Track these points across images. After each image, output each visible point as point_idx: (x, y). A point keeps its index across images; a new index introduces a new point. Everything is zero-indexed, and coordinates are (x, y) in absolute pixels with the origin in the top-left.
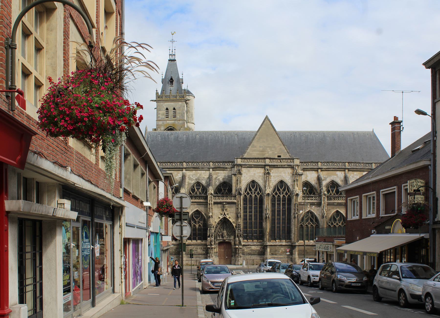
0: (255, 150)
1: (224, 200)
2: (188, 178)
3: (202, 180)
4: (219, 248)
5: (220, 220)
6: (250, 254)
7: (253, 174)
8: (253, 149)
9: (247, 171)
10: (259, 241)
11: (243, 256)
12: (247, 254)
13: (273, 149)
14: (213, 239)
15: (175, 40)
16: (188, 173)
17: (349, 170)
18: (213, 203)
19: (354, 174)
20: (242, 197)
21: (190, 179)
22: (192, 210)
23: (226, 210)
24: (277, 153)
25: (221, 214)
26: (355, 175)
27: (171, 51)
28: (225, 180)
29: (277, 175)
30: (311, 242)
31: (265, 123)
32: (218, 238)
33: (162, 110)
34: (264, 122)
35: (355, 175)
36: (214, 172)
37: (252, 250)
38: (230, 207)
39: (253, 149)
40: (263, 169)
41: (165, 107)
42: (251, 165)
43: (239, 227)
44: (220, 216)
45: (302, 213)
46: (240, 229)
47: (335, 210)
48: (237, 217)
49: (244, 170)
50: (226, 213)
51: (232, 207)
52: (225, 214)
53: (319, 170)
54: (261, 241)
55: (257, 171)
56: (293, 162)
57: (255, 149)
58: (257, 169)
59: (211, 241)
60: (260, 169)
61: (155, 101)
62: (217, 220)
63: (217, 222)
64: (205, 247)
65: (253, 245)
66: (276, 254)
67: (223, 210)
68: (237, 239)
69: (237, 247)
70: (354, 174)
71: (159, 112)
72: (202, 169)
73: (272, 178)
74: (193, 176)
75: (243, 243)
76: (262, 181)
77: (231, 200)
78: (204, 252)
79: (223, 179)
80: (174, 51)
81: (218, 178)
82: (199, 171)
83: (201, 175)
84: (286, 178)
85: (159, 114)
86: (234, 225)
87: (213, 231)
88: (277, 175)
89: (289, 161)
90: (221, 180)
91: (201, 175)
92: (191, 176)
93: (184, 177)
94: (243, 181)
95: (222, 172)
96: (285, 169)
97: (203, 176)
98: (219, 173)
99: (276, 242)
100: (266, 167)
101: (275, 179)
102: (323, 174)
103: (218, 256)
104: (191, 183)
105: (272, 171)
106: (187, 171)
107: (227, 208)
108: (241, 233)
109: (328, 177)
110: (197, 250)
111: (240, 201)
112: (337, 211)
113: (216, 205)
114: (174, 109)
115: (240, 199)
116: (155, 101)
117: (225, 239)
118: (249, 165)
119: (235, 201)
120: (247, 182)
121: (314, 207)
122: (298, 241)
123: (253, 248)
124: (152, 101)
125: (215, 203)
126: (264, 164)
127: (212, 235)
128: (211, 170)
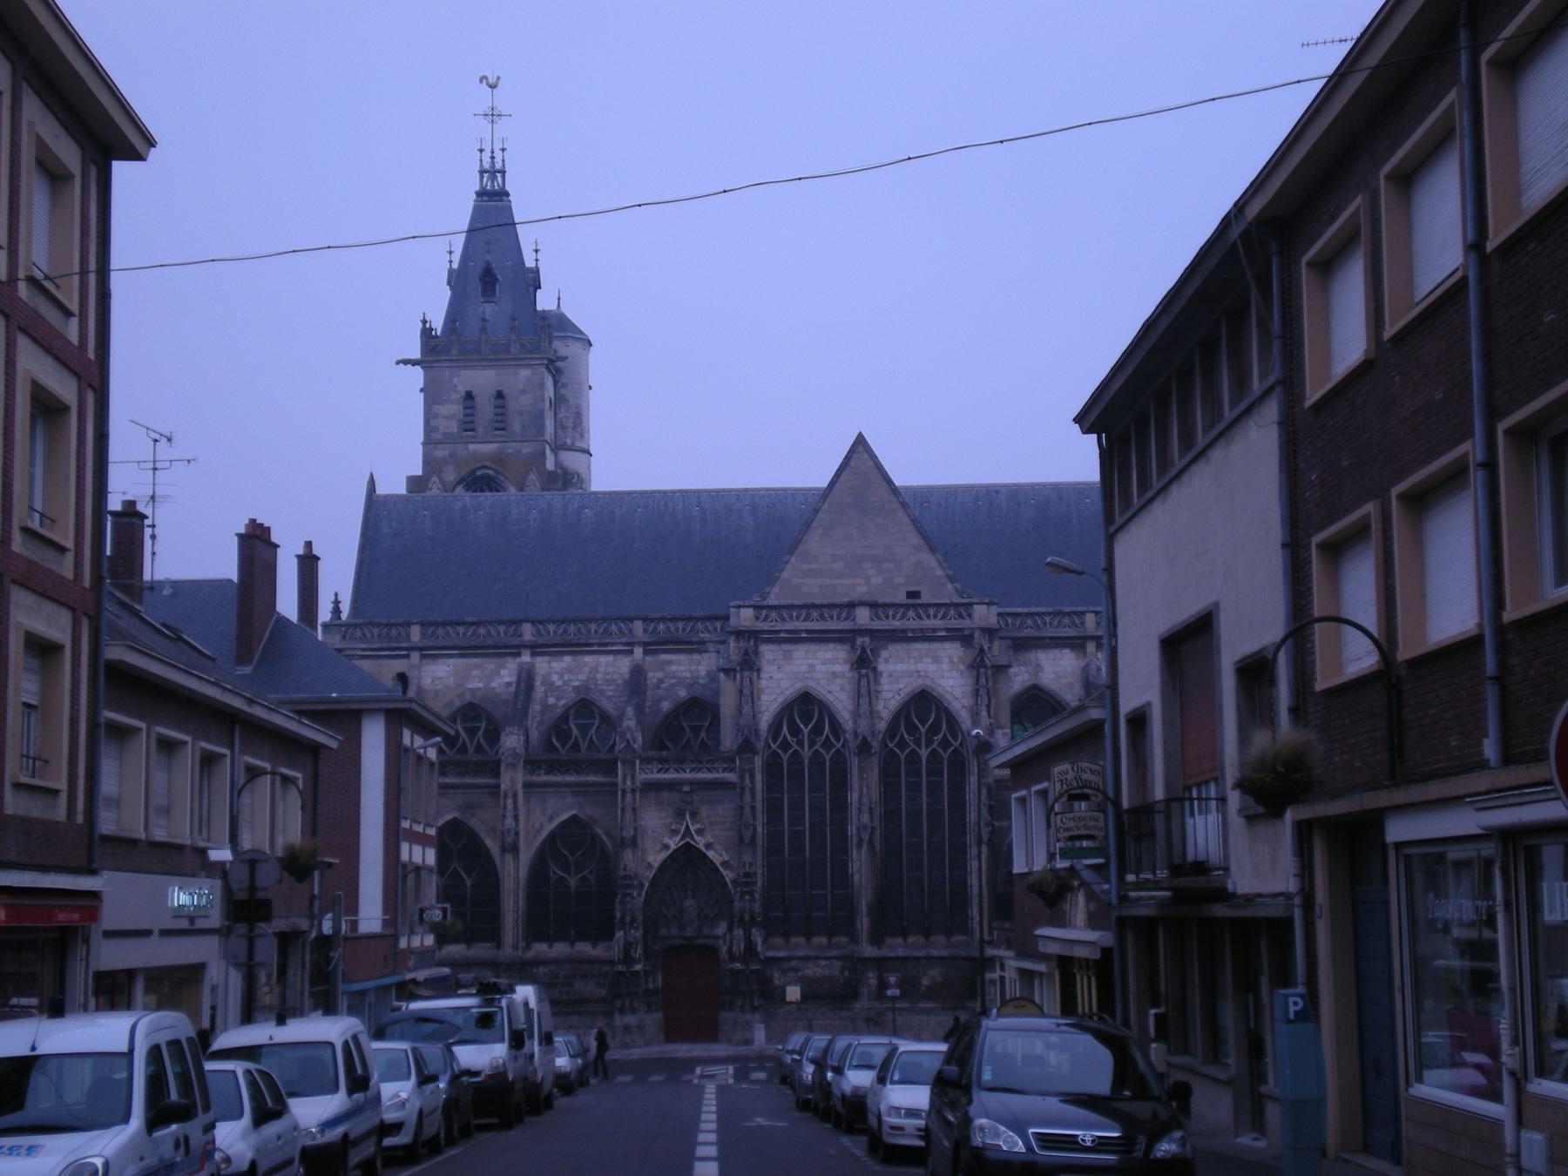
8: (805, 566)
16: (542, 665)
20: (758, 762)
22: (551, 819)
25: (675, 832)
39: (805, 566)
44: (667, 840)
50: (692, 829)
55: (820, 655)
58: (823, 647)
60: (831, 646)
63: (656, 865)
67: (680, 814)
73: (884, 680)
78: (603, 992)
84: (943, 682)
92: (555, 678)
96: (936, 645)
105: (884, 654)
119: (732, 777)
120: (781, 699)
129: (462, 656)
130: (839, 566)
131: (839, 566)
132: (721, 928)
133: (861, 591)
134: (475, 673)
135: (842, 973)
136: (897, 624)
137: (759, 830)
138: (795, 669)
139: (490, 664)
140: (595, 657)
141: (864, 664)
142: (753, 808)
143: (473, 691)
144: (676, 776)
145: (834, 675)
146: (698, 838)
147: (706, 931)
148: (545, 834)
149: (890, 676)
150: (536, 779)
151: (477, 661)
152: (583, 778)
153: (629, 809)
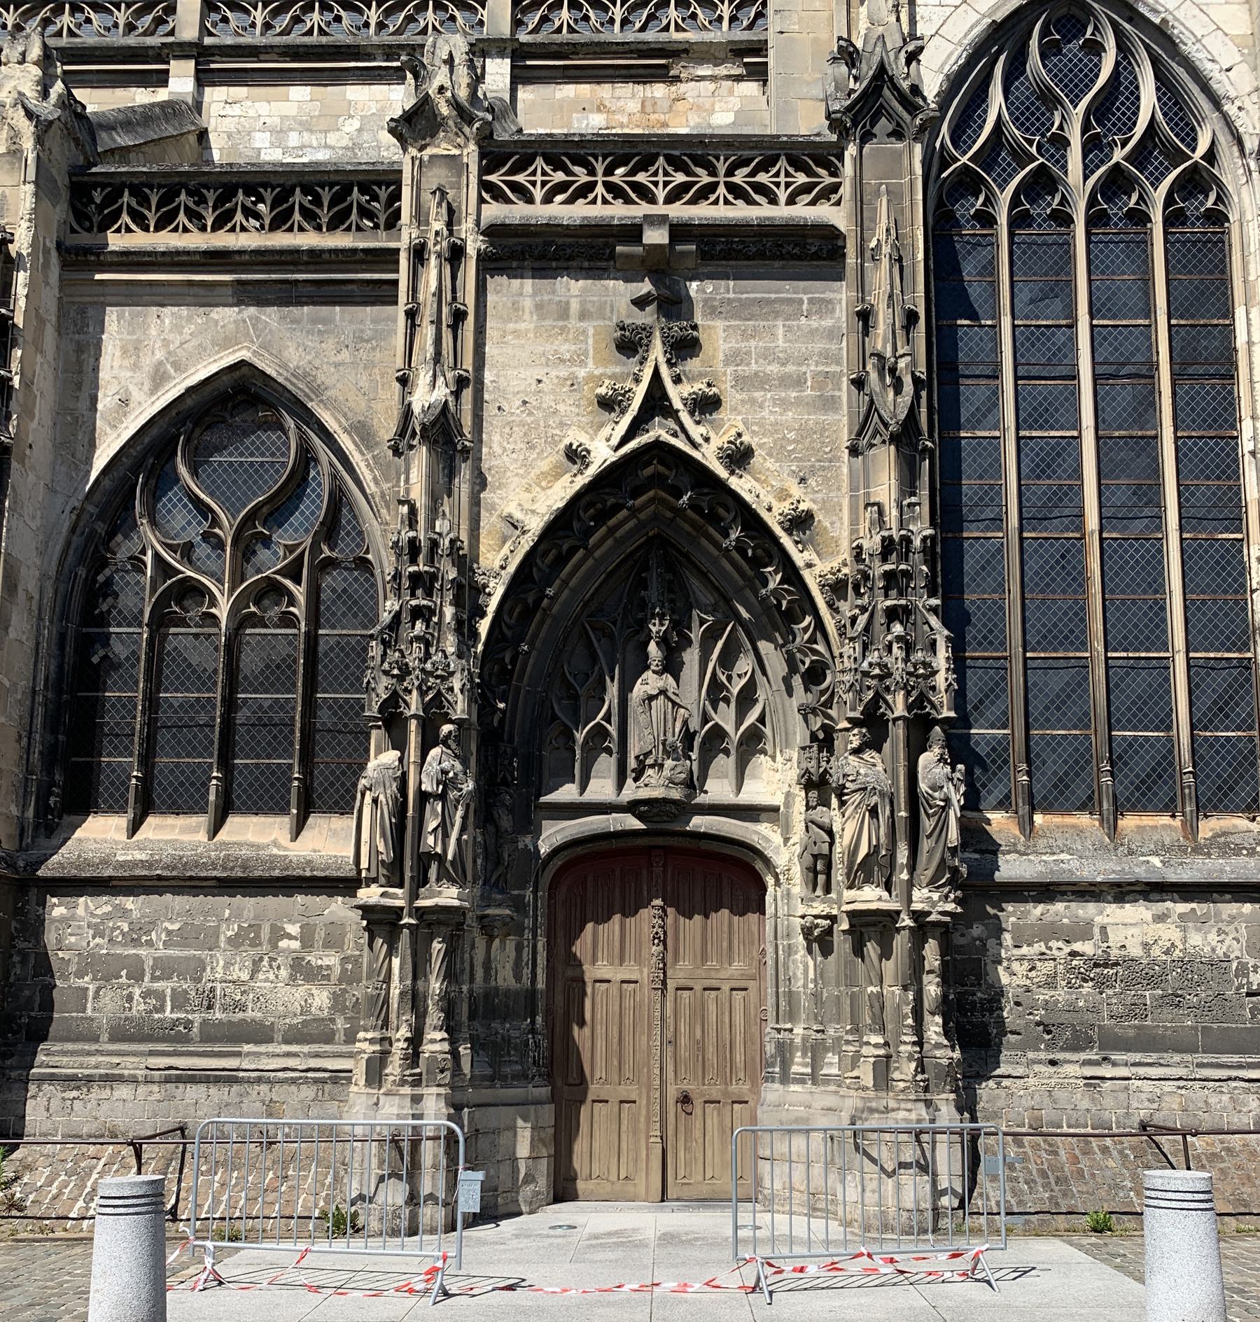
10: (1209, 827)
18: (474, 245)
23: (684, 347)
25: (608, 404)
38: (740, 310)
44: (576, 437)
50: (676, 394)
51: (769, 309)
52: (656, 403)
63: (536, 525)
65: (1123, 892)
67: (630, 344)
78: (321, 999)
123: (1130, 927)
125: (518, 252)
132: (773, 779)
144: (618, 211)
146: (696, 432)
147: (718, 789)
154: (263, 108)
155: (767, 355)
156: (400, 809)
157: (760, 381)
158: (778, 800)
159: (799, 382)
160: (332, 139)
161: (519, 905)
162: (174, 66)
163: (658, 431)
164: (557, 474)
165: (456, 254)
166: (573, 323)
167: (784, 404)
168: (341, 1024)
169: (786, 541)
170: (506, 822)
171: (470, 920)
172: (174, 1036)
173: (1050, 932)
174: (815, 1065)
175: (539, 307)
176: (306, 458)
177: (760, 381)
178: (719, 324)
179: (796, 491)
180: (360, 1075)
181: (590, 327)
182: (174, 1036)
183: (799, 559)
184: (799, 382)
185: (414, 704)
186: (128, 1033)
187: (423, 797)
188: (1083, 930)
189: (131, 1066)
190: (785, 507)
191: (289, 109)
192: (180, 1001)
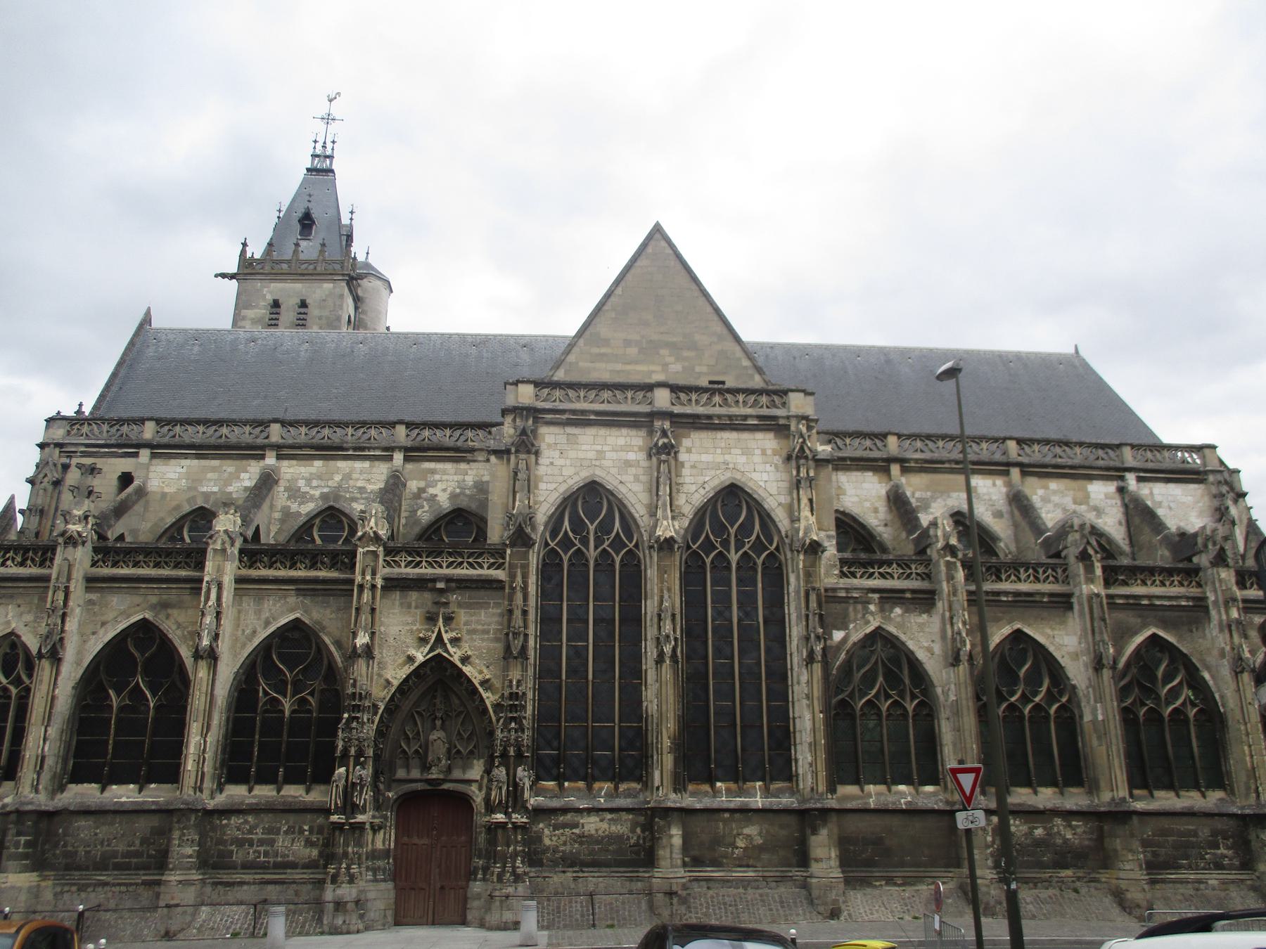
0: (602, 357)
1: (438, 571)
2: (287, 489)
3: (354, 499)
4: (403, 829)
5: (415, 673)
6: (570, 862)
7: (591, 455)
8: (595, 350)
9: (562, 439)
10: (622, 787)
11: (533, 871)
12: (555, 863)
13: (686, 354)
14: (366, 773)
15: (335, 113)
16: (290, 470)
17: (1027, 470)
18: (379, 582)
19: (1046, 488)
20: (534, 559)
21: (294, 493)
22: (267, 623)
23: (449, 619)
24: (704, 369)
25: (423, 641)
26: (1055, 492)
27: (319, 146)
28: (463, 503)
29: (709, 462)
30: (902, 794)
31: (649, 250)
32: (401, 773)
33: (256, 307)
34: (644, 245)
35: (1055, 492)
36: (409, 466)
37: (582, 839)
38: (468, 606)
39: (595, 350)
40: (643, 433)
41: (270, 298)
42: (583, 412)
43: (513, 708)
44: (412, 652)
45: (845, 640)
46: (518, 720)
47: (1006, 630)
48: (511, 655)
49: (549, 437)
50: (446, 637)
52: (439, 638)
53: (895, 469)
54: (634, 785)
55: (611, 440)
56: (784, 404)
57: (603, 350)
58: (614, 431)
59: (350, 788)
60: (624, 431)
61: (232, 277)
62: (397, 674)
63: (396, 683)
64: (321, 820)
65: (589, 811)
66: (716, 863)
67: (431, 619)
68: (500, 773)
69: (500, 817)
70: (1046, 488)
71: (244, 312)
72: (359, 452)
73: (686, 471)
74: (308, 481)
75: (533, 801)
76: (638, 488)
77: (480, 571)
78: (315, 853)
79: (453, 496)
80: (329, 146)
81: (431, 491)
82: (341, 464)
83: (347, 477)
84: (755, 476)
85: (244, 318)
86: (489, 698)
87: (369, 730)
88: (709, 462)
89: (764, 399)
90: (444, 502)
91: (347, 477)
92: (301, 483)
93: (267, 482)
94: (542, 486)
95: (448, 466)
96: (745, 435)
97: (360, 484)
98: (433, 472)
99: (716, 793)
100: (658, 424)
101: (701, 480)
102: (914, 487)
103: (395, 877)
104: (299, 514)
105: (686, 442)
106: (285, 463)
107: (453, 607)
108: (526, 737)
109: (934, 498)
110: (272, 843)
111: (525, 577)
112: (1018, 635)
113: (397, 595)
114: (303, 304)
115: (525, 567)
116: (232, 277)
117: (434, 774)
118: (574, 412)
119: (500, 574)
120: (562, 488)
121: (898, 611)
122: (832, 789)
123: (592, 824)
124: (223, 276)
125: (393, 584)
126: (645, 408)
127: (360, 753)
128: (398, 457)
129: (199, 457)
130: (633, 351)
131: (633, 351)
132: (476, 771)
133: (659, 377)
134: (210, 475)
135: (633, 831)
136: (700, 410)
137: (531, 642)
138: (581, 455)
139: (229, 467)
140: (349, 463)
141: (664, 453)
142: (525, 613)
143: (206, 496)
144: (430, 571)
145: (628, 464)
146: (452, 650)
147: (457, 774)
148: (256, 642)
149: (693, 467)
150: (254, 573)
151: (216, 463)
152: (313, 574)
153: (367, 609)
154: (303, 469)
155: (478, 622)
156: (346, 787)
157: (473, 632)
158: (478, 778)
159: (488, 632)
160: (330, 483)
161: (385, 817)
162: (268, 453)
163: (439, 651)
164: (404, 664)
165: (374, 587)
166: (413, 610)
167: (483, 640)
168: (322, 862)
169: (481, 690)
170: (381, 786)
171: (367, 826)
172: (263, 867)
173: (564, 826)
174: (484, 875)
175: (401, 604)
176: (319, 650)
177: (473, 632)
178: (462, 611)
179: (485, 671)
180: (329, 881)
181: (418, 611)
182: (263, 867)
183: (485, 695)
184: (488, 632)
185: (353, 751)
186: (248, 866)
187: (354, 784)
188: (576, 826)
189: (247, 878)
190: (480, 677)
191: (313, 470)
192: (266, 854)
